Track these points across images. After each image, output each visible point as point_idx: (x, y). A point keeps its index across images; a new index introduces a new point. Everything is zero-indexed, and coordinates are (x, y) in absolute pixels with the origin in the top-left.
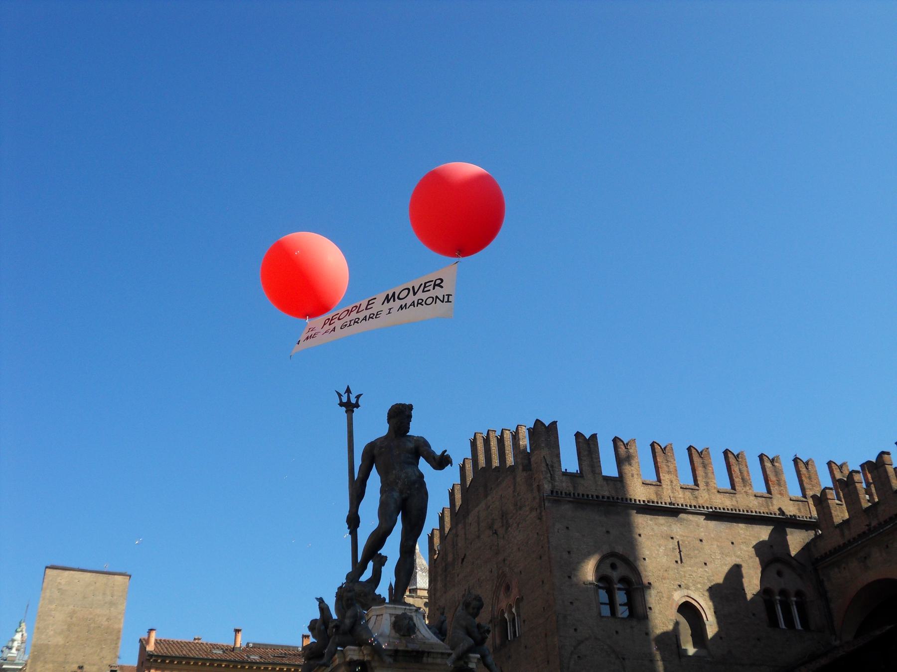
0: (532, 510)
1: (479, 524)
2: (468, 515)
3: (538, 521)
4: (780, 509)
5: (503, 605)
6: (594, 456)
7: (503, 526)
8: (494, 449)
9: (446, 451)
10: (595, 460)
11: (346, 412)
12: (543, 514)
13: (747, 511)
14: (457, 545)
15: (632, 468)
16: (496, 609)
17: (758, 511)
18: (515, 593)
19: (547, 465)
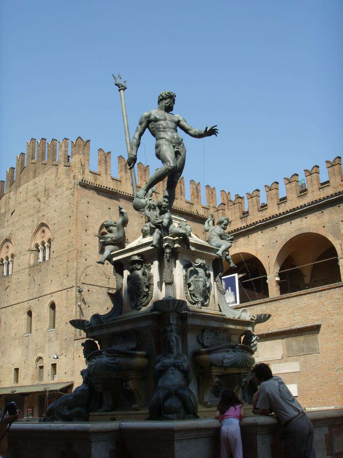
0: (67, 190)
1: (27, 193)
2: (20, 187)
3: (71, 196)
4: (197, 210)
5: (39, 242)
6: (107, 164)
7: (45, 196)
8: (44, 150)
9: (216, 126)
10: (108, 167)
11: (119, 90)
12: (76, 192)
13: (181, 209)
14: (8, 204)
15: (127, 175)
16: (33, 243)
17: (186, 210)
18: (48, 235)
19: (82, 165)
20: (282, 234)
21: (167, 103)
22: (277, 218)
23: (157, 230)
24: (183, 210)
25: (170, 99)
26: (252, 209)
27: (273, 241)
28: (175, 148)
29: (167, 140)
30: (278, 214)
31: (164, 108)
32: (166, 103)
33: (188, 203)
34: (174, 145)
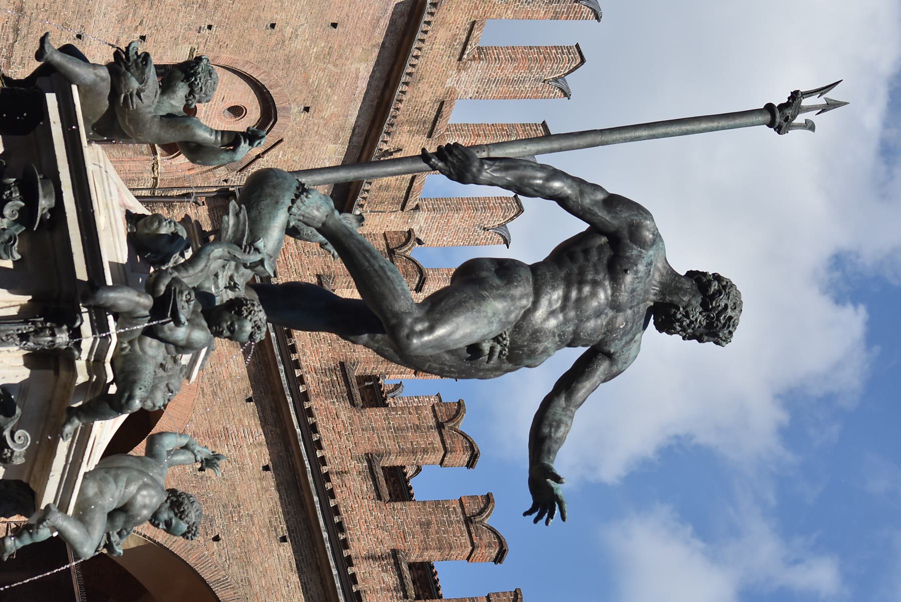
9: (563, 518)
11: (769, 107)
13: (410, 74)
20: (251, 572)
21: (687, 312)
22: (328, 545)
23: (147, 301)
24: (405, 88)
25: (704, 324)
26: (385, 424)
27: (218, 521)
28: (496, 343)
29: (529, 312)
30: (351, 552)
31: (668, 299)
32: (689, 309)
33: (439, 111)
34: (504, 339)
